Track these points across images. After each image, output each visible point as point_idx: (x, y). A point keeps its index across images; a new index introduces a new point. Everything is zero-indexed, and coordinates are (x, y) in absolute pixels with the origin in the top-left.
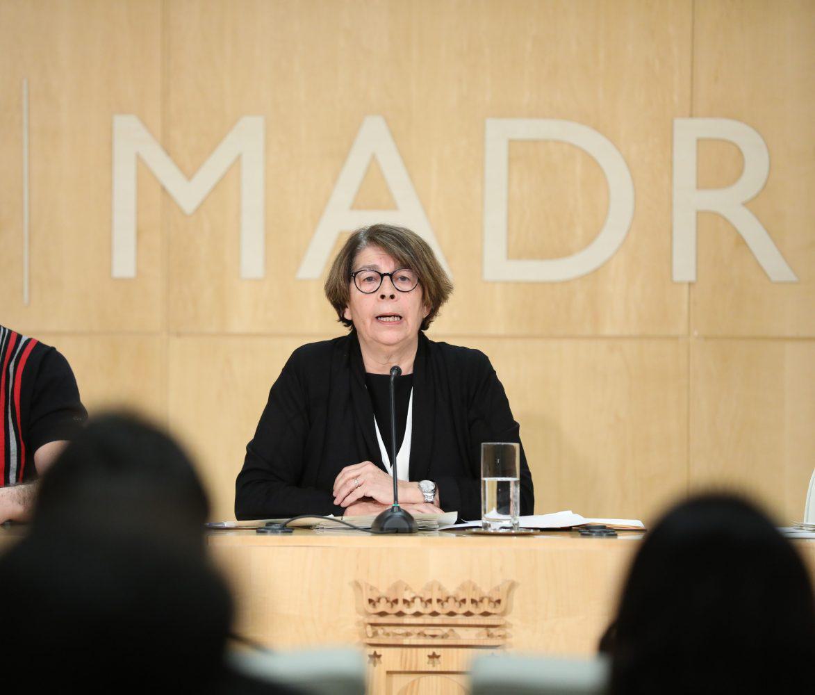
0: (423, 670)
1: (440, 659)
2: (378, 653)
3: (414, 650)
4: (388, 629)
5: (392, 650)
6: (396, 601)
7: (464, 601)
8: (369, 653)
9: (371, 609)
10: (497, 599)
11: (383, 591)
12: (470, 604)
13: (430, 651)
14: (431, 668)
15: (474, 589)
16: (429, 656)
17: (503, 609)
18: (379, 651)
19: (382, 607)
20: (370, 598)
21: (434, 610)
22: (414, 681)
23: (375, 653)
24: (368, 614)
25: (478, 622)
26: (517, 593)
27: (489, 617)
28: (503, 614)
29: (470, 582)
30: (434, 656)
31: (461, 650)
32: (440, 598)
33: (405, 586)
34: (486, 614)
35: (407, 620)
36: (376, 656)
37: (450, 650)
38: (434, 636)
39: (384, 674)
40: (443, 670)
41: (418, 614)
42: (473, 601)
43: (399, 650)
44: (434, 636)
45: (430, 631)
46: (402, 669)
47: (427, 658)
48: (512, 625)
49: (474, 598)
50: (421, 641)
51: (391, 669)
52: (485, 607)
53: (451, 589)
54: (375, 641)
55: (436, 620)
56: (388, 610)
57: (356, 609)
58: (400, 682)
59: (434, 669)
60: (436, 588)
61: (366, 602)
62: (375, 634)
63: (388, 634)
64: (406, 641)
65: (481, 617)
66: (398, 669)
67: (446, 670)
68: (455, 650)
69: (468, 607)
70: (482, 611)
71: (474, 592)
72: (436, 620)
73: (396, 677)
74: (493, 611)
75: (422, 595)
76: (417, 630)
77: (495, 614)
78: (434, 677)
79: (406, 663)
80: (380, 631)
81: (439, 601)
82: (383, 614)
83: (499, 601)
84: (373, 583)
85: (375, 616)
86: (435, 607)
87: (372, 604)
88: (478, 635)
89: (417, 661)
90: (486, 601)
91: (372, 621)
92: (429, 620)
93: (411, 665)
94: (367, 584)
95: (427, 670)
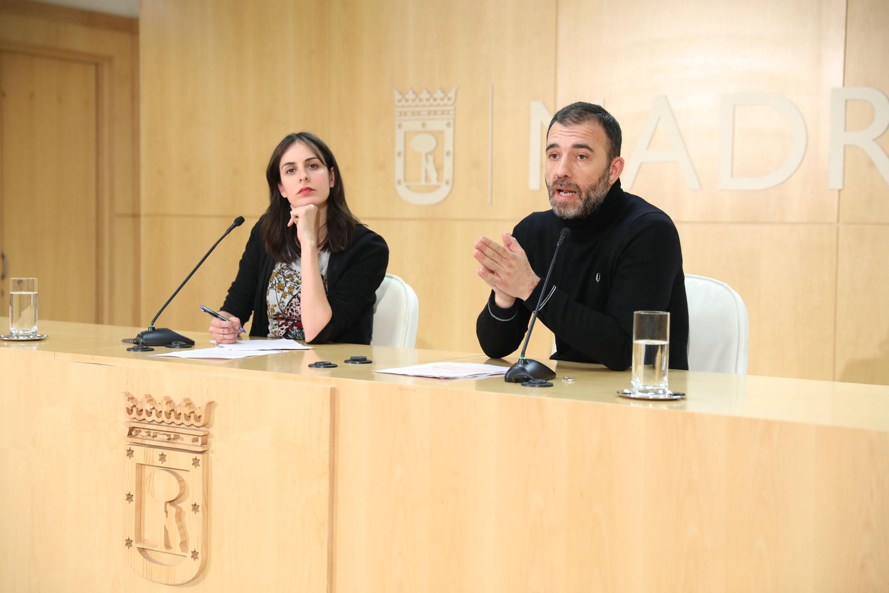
3: (152, 449)
8: (126, 449)
13: (160, 451)
14: (160, 464)
18: (134, 448)
22: (151, 474)
31: (178, 452)
35: (148, 426)
36: (130, 453)
50: (155, 443)
60: (165, 402)
62: (130, 434)
64: (147, 442)
77: (203, 426)
84: (135, 395)
94: (127, 394)
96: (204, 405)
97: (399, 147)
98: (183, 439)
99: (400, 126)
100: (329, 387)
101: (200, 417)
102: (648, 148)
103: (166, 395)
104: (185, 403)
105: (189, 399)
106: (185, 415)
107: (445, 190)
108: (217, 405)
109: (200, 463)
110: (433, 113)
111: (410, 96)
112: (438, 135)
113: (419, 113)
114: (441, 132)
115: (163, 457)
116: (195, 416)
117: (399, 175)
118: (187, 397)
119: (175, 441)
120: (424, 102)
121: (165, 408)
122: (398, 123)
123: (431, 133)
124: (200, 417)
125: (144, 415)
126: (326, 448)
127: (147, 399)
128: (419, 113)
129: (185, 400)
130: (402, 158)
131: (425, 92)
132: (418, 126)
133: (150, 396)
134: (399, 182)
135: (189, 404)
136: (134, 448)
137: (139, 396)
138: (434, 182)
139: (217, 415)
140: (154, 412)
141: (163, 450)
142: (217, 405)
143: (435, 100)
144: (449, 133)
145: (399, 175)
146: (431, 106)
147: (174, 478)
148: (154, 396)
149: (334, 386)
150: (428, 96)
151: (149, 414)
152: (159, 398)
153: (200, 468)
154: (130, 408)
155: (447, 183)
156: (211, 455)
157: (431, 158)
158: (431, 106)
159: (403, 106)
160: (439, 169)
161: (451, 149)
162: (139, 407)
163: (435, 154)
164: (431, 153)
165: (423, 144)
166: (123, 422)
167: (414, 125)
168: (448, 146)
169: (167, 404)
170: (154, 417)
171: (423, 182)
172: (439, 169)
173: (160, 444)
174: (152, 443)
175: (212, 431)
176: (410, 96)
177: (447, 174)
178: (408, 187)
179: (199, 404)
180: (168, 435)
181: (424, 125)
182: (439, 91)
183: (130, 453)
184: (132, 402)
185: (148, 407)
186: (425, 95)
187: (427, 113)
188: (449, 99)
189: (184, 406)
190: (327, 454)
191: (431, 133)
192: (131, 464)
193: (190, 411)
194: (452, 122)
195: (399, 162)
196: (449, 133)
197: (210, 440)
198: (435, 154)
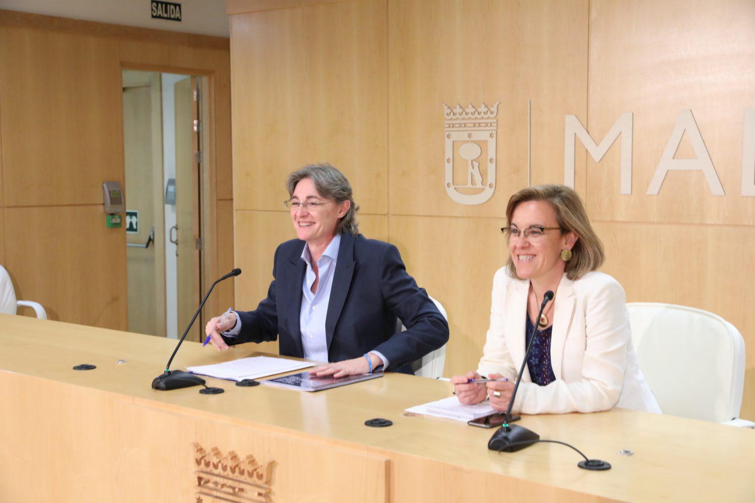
2: (201, 498)
3: (219, 500)
18: (203, 497)
50: (222, 495)
55: (230, 483)
60: (229, 458)
62: (200, 484)
64: (215, 493)
72: (230, 483)
77: (266, 483)
84: (203, 446)
96: (266, 465)
97: (449, 154)
99: (448, 136)
100: (384, 459)
101: (262, 475)
102: (673, 158)
103: (231, 449)
104: (248, 461)
105: (252, 456)
106: (248, 472)
107: (489, 192)
110: (478, 125)
111: (458, 110)
112: (482, 145)
114: (485, 142)
116: (258, 474)
117: (448, 178)
118: (250, 453)
119: (241, 494)
121: (230, 463)
122: (447, 133)
123: (476, 142)
124: (262, 475)
125: (211, 467)
127: (213, 453)
130: (451, 164)
131: (470, 106)
132: (464, 136)
133: (216, 449)
134: (448, 185)
135: (252, 462)
136: (203, 497)
137: (208, 449)
140: (220, 465)
144: (492, 143)
145: (448, 178)
146: (476, 118)
148: (221, 449)
149: (388, 458)
151: (216, 467)
152: (225, 452)
154: (199, 459)
155: (491, 186)
157: (476, 164)
158: (476, 118)
159: (451, 119)
160: (483, 174)
161: (494, 157)
162: (207, 459)
163: (480, 161)
164: (475, 160)
165: (469, 152)
166: (192, 471)
167: (459, 135)
168: (491, 154)
169: (232, 459)
170: (219, 471)
171: (469, 185)
172: (483, 174)
173: (226, 496)
174: (219, 494)
175: (274, 488)
176: (458, 110)
177: (491, 179)
179: (262, 461)
181: (469, 136)
182: (483, 106)
184: (201, 453)
185: (215, 460)
186: (470, 110)
188: (492, 113)
191: (476, 142)
195: (448, 167)
196: (492, 143)
197: (273, 497)
198: (480, 161)
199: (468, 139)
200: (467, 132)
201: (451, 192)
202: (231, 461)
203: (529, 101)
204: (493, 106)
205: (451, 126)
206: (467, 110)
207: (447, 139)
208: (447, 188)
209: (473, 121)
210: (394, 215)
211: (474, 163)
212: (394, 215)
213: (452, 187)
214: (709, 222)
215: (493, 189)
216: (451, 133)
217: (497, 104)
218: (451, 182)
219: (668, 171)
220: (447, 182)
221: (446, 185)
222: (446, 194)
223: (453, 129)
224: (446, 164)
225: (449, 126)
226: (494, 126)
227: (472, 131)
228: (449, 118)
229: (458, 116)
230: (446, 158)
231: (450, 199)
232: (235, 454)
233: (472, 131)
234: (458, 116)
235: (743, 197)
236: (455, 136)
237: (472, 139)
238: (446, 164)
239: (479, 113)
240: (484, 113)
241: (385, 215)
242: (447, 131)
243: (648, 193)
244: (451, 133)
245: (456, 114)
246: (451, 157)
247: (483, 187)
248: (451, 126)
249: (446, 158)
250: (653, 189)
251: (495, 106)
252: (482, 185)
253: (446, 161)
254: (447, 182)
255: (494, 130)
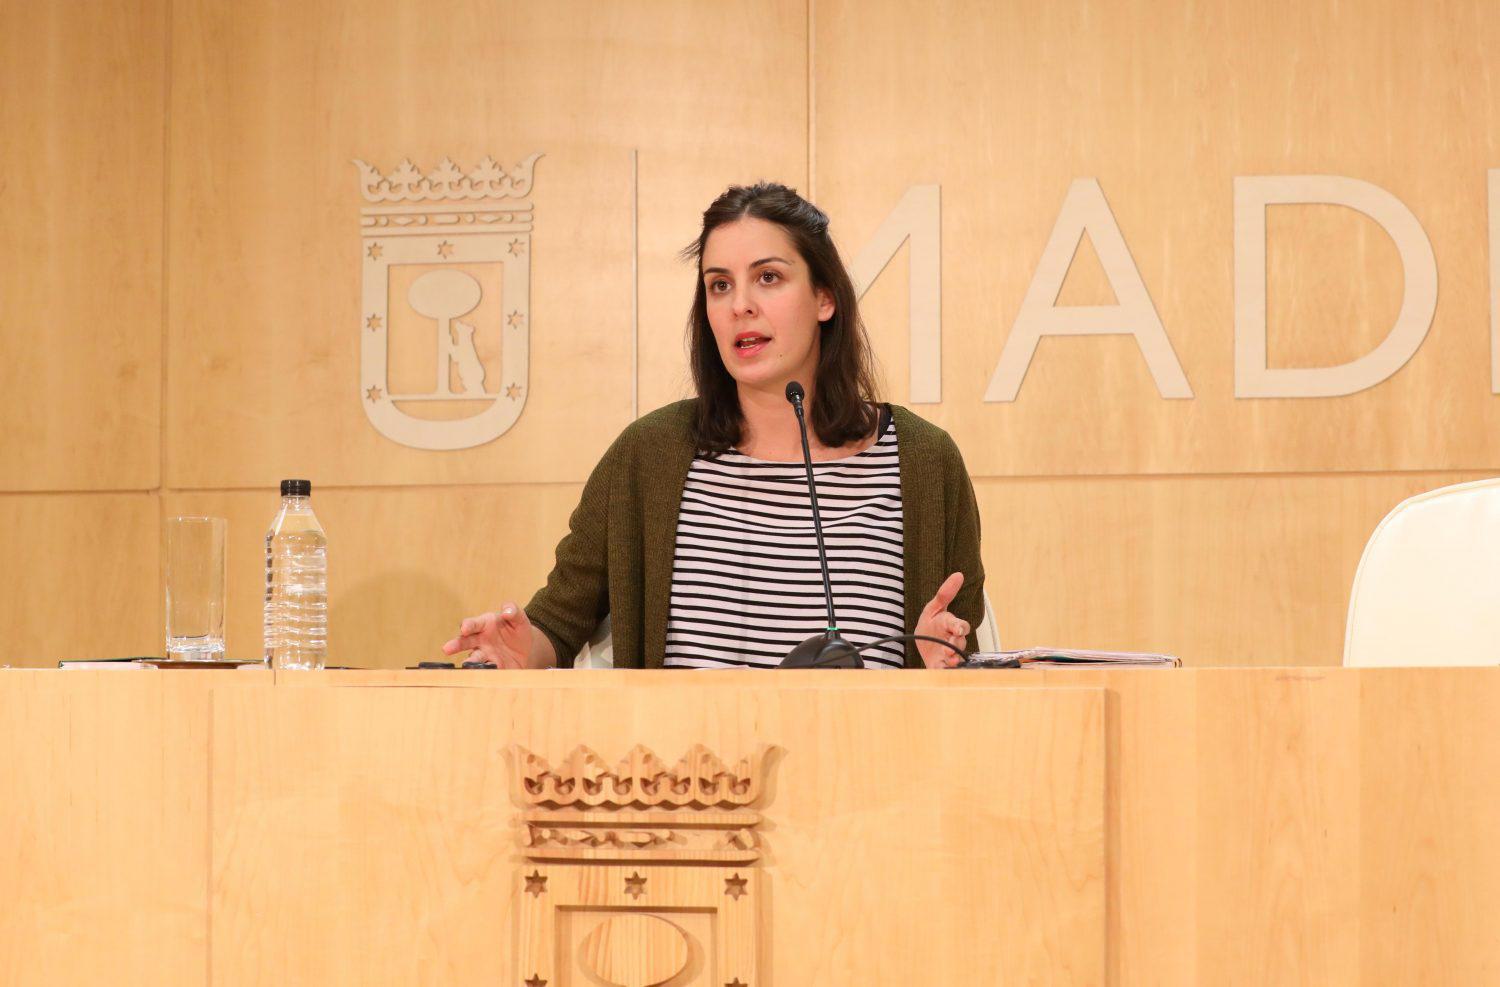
0: (617, 903)
1: (644, 886)
2: (541, 874)
3: (602, 868)
4: (564, 832)
5: (566, 868)
6: (571, 781)
7: (687, 781)
8: (526, 874)
9: (530, 798)
10: (744, 777)
11: (556, 765)
12: (698, 788)
14: (629, 900)
15: (706, 758)
16: (628, 880)
17: (753, 798)
18: (543, 870)
19: (548, 792)
20: (529, 777)
21: (636, 797)
23: (536, 872)
24: (530, 807)
25: (717, 820)
26: (783, 771)
27: (735, 811)
28: (756, 804)
29: (700, 748)
30: (635, 882)
31: (681, 869)
32: (646, 777)
33: (586, 755)
34: (725, 805)
35: (589, 817)
36: (536, 882)
37: (663, 869)
38: (640, 845)
39: (551, 911)
40: (650, 904)
41: (608, 805)
42: (704, 783)
43: (577, 868)
44: (640, 845)
45: (625, 836)
46: (582, 903)
47: (623, 881)
48: (775, 825)
49: (704, 777)
51: (563, 903)
52: (724, 793)
53: (670, 762)
54: (536, 852)
55: (641, 817)
56: (558, 799)
57: (511, 796)
58: (582, 926)
59: (636, 903)
60: (639, 758)
61: (520, 785)
63: (565, 841)
64: (589, 853)
65: (720, 811)
66: (574, 901)
67: (656, 904)
68: (671, 869)
69: (695, 792)
70: (718, 800)
71: (704, 765)
72: (641, 817)
73: (576, 916)
74: (736, 800)
75: (614, 772)
76: (600, 834)
77: (746, 805)
78: (636, 917)
79: (587, 892)
80: (546, 833)
81: (645, 783)
82: (550, 805)
83: (747, 782)
84: (537, 752)
85: (540, 809)
86: (638, 793)
87: (535, 789)
88: (718, 846)
89: (606, 890)
90: (724, 782)
91: (531, 817)
92: (628, 815)
93: (596, 894)
94: (523, 750)
95: (623, 904)
97: (373, 303)
98: (684, 841)
102: (1055, 304)
107: (505, 411)
108: (786, 752)
109: (748, 887)
113: (428, 219)
115: (635, 882)
117: (373, 372)
120: (445, 190)
121: (639, 772)
122: (370, 243)
125: (579, 788)
126: (1093, 819)
128: (428, 219)
129: (700, 748)
130: (381, 332)
131: (446, 166)
132: (428, 249)
133: (584, 749)
134: (373, 393)
138: (474, 390)
139: (783, 773)
141: (637, 869)
142: (786, 752)
143: (473, 185)
147: (673, 929)
150: (456, 176)
153: (748, 900)
155: (511, 391)
156: (769, 870)
157: (463, 331)
161: (524, 311)
171: (443, 392)
173: (627, 854)
175: (768, 813)
176: (406, 176)
177: (512, 371)
178: (393, 402)
180: (650, 834)
181: (443, 248)
183: (536, 882)
184: (539, 764)
186: (446, 175)
187: (454, 219)
189: (699, 762)
190: (1101, 835)
192: (537, 910)
193: (717, 772)
194: (524, 238)
195: (372, 344)
197: (766, 836)
199: (440, 259)
200: (435, 239)
201: (382, 415)
202: (646, 766)
203: (634, 154)
204: (519, 166)
205: (383, 221)
206: (435, 177)
207: (367, 261)
208: (367, 404)
209: (452, 208)
210: (181, 490)
211: (458, 326)
212: (181, 490)
213: (385, 400)
214: (1152, 468)
215: (520, 402)
216: (380, 242)
217: (532, 159)
218: (381, 384)
219: (1041, 337)
220: (366, 385)
221: (365, 394)
222: (363, 415)
223: (390, 230)
224: (366, 332)
225: (376, 224)
226: (524, 222)
227: (449, 234)
228: (376, 198)
229: (404, 192)
230: (367, 312)
231: (379, 434)
232: (647, 752)
233: (449, 234)
234: (404, 192)
235: (1239, 399)
236: (392, 250)
237: (450, 259)
238: (366, 332)
239: (473, 185)
240: (491, 182)
241: (147, 492)
242: (367, 237)
243: (987, 398)
244: (380, 242)
245: (399, 185)
246: (381, 312)
247: (489, 396)
248: (383, 221)
249: (367, 312)
250: (1002, 387)
251: (528, 164)
252: (486, 391)
253: (365, 322)
254: (366, 385)
255: (521, 232)
